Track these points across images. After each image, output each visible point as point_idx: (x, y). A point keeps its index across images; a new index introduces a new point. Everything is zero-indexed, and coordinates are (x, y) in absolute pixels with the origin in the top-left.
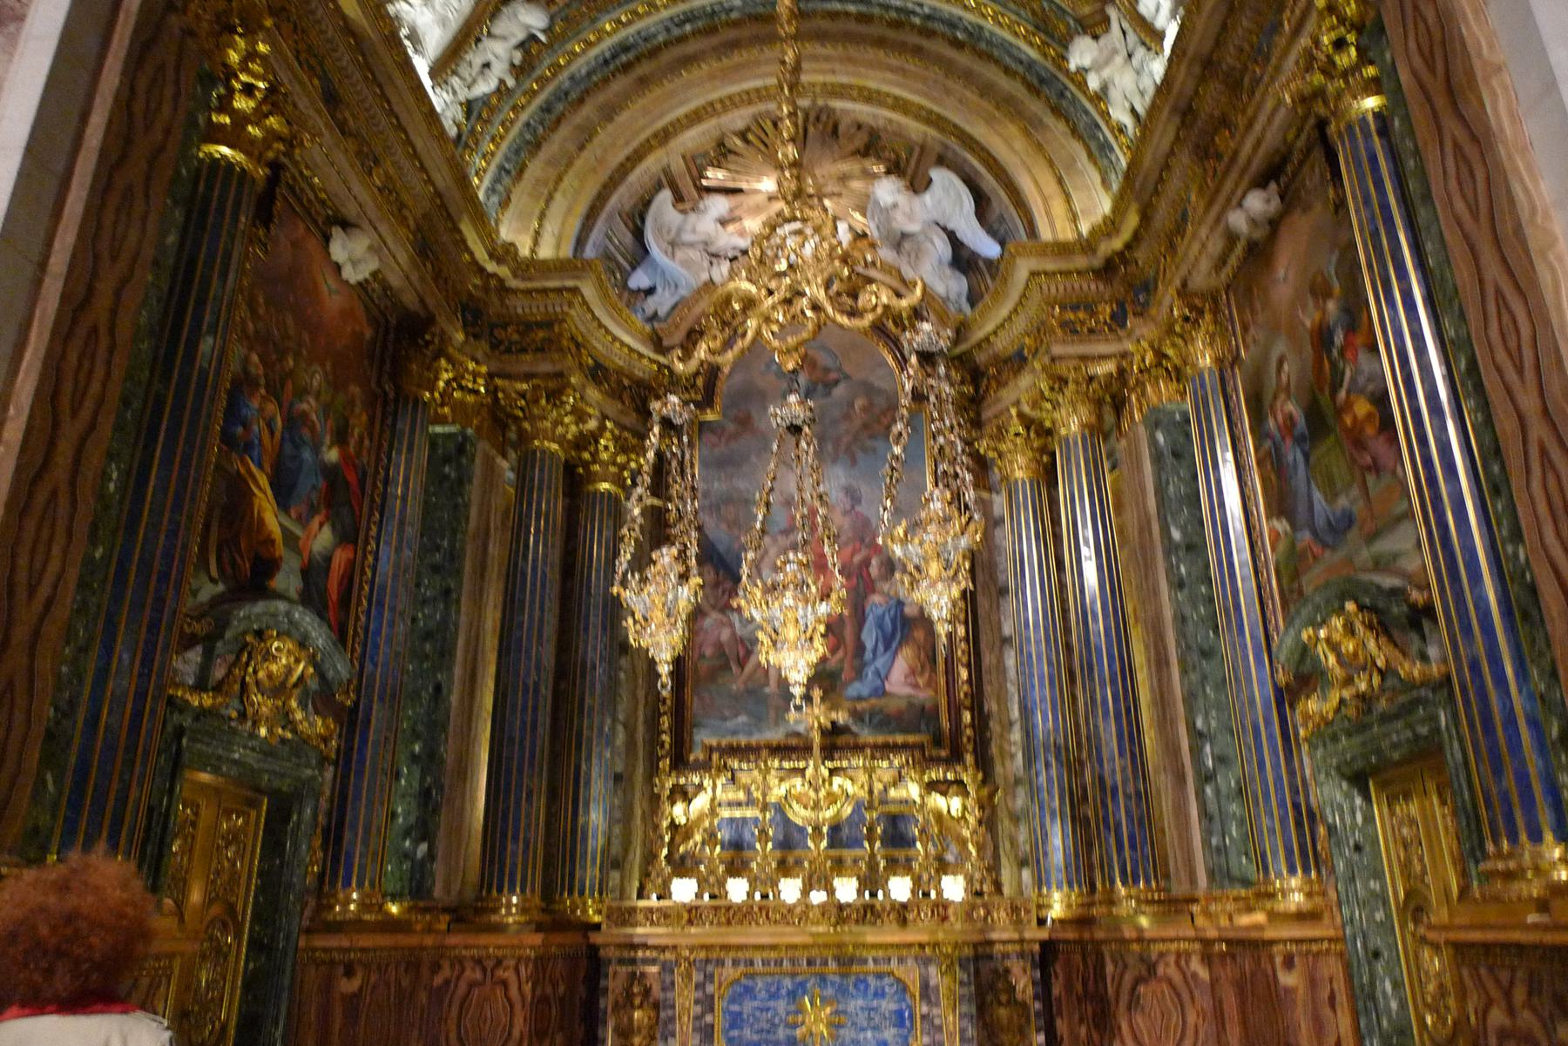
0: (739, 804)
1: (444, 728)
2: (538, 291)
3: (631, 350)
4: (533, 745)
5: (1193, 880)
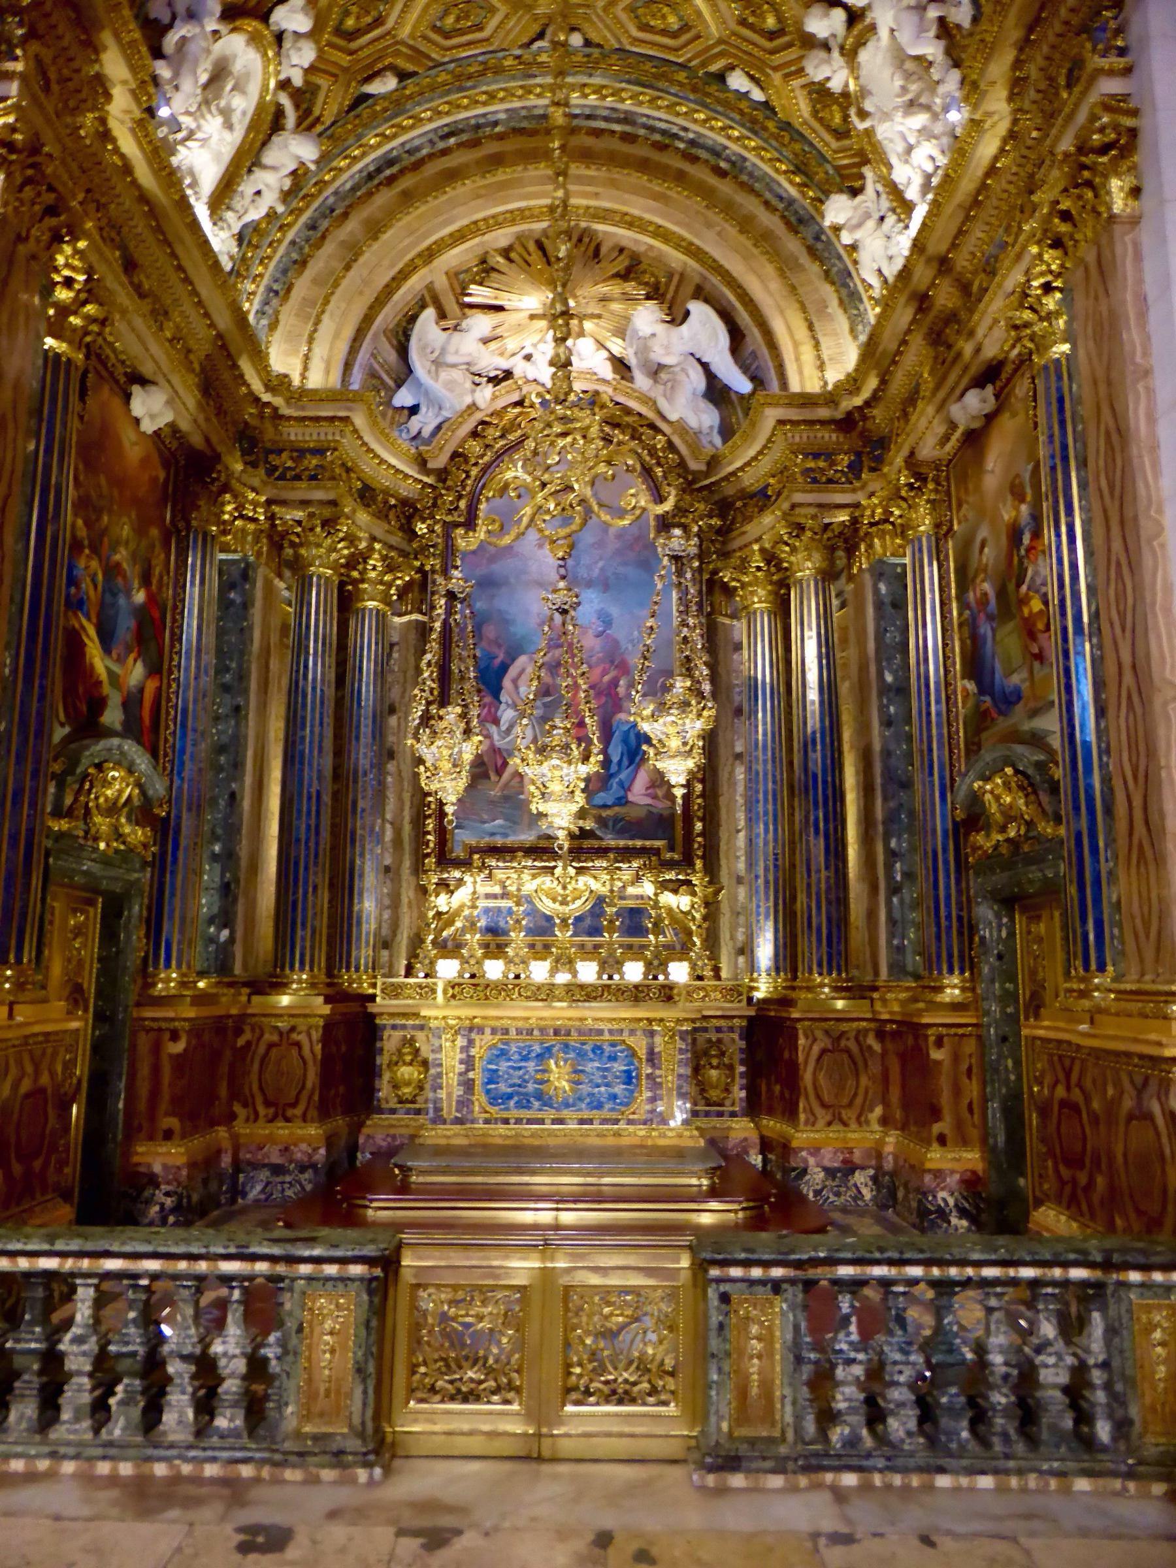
0: (495, 896)
1: (239, 830)
2: (311, 419)
3: (398, 471)
4: (317, 844)
5: (876, 973)
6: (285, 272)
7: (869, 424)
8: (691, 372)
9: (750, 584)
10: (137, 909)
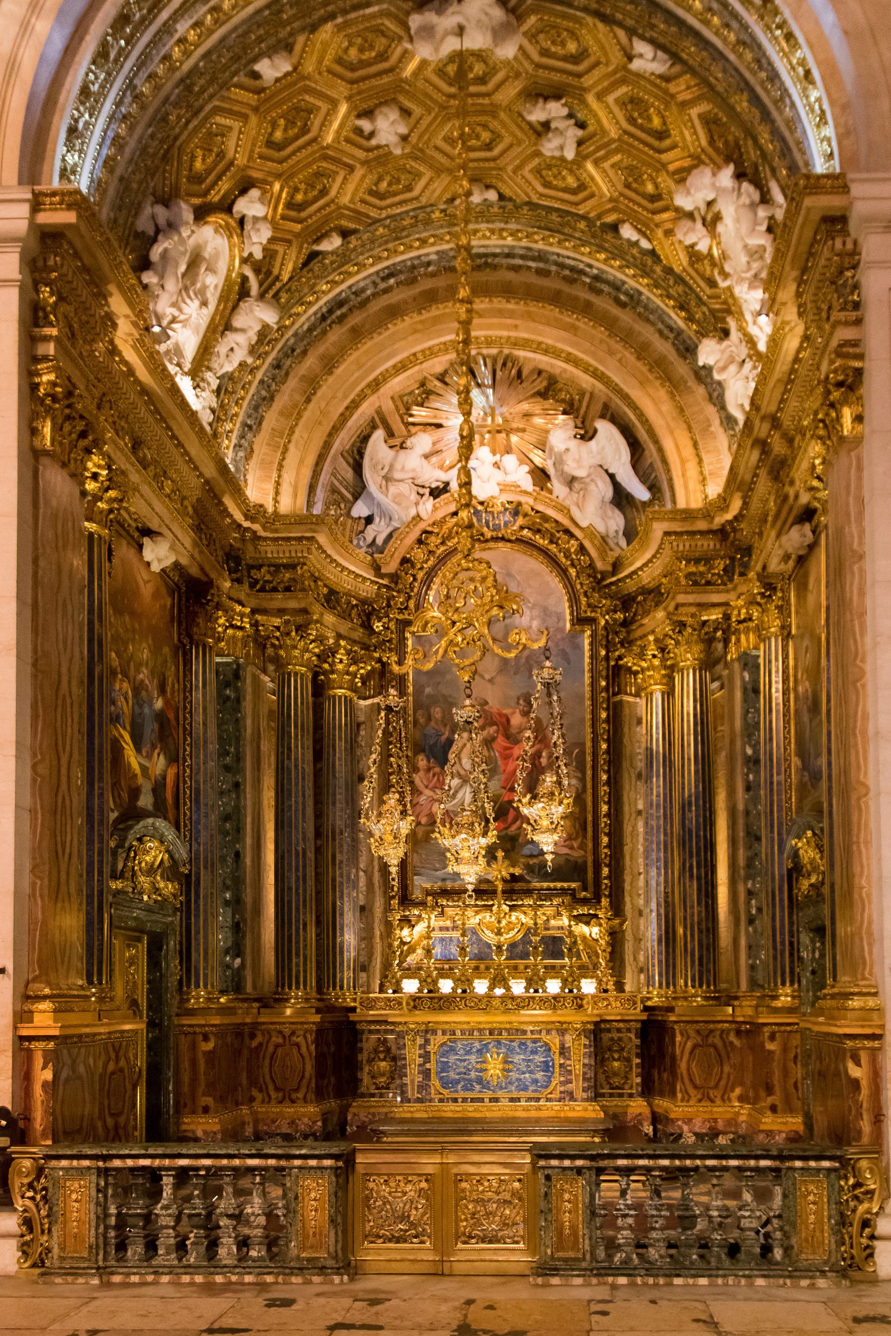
2: (283, 539)
5: (738, 987)
6: (256, 408)
7: (738, 536)
8: (599, 483)
9: (648, 669)
10: (172, 943)
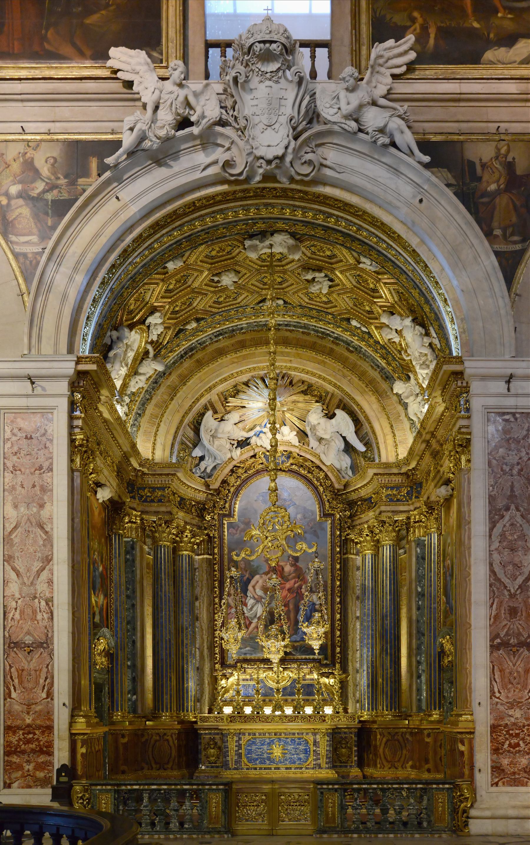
3: (196, 489)
4: (170, 661)
